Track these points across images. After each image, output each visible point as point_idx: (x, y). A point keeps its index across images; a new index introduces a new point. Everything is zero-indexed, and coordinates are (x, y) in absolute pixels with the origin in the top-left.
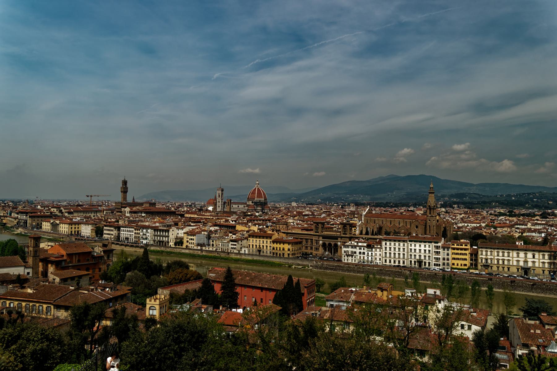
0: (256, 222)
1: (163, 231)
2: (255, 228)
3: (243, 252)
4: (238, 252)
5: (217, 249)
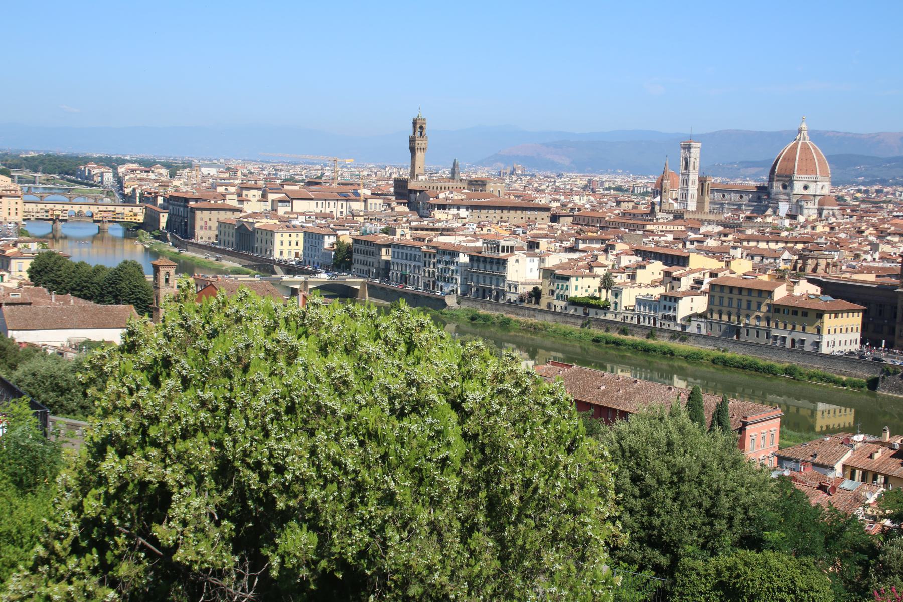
0: (762, 245)
1: (491, 261)
2: (742, 266)
3: (692, 328)
4: (679, 329)
5: (625, 318)
